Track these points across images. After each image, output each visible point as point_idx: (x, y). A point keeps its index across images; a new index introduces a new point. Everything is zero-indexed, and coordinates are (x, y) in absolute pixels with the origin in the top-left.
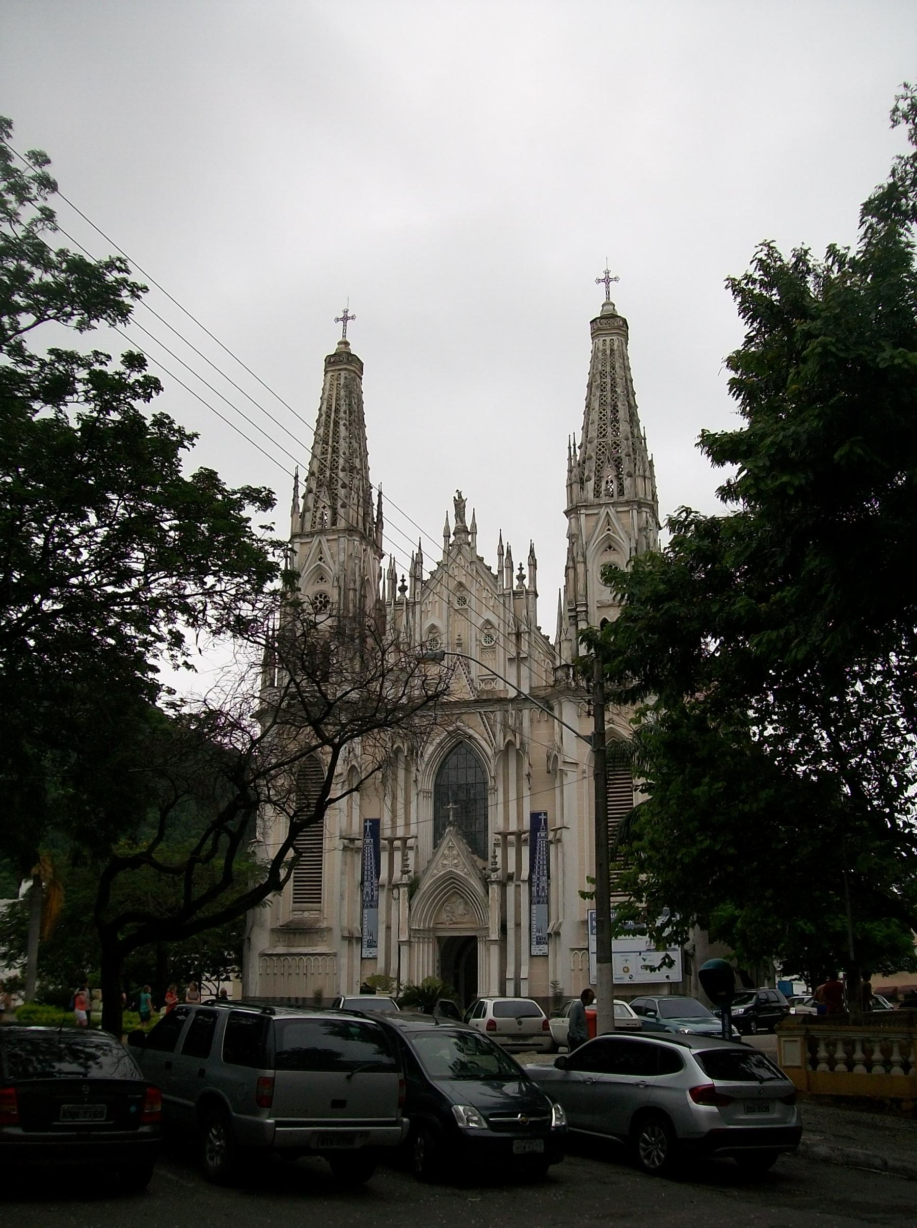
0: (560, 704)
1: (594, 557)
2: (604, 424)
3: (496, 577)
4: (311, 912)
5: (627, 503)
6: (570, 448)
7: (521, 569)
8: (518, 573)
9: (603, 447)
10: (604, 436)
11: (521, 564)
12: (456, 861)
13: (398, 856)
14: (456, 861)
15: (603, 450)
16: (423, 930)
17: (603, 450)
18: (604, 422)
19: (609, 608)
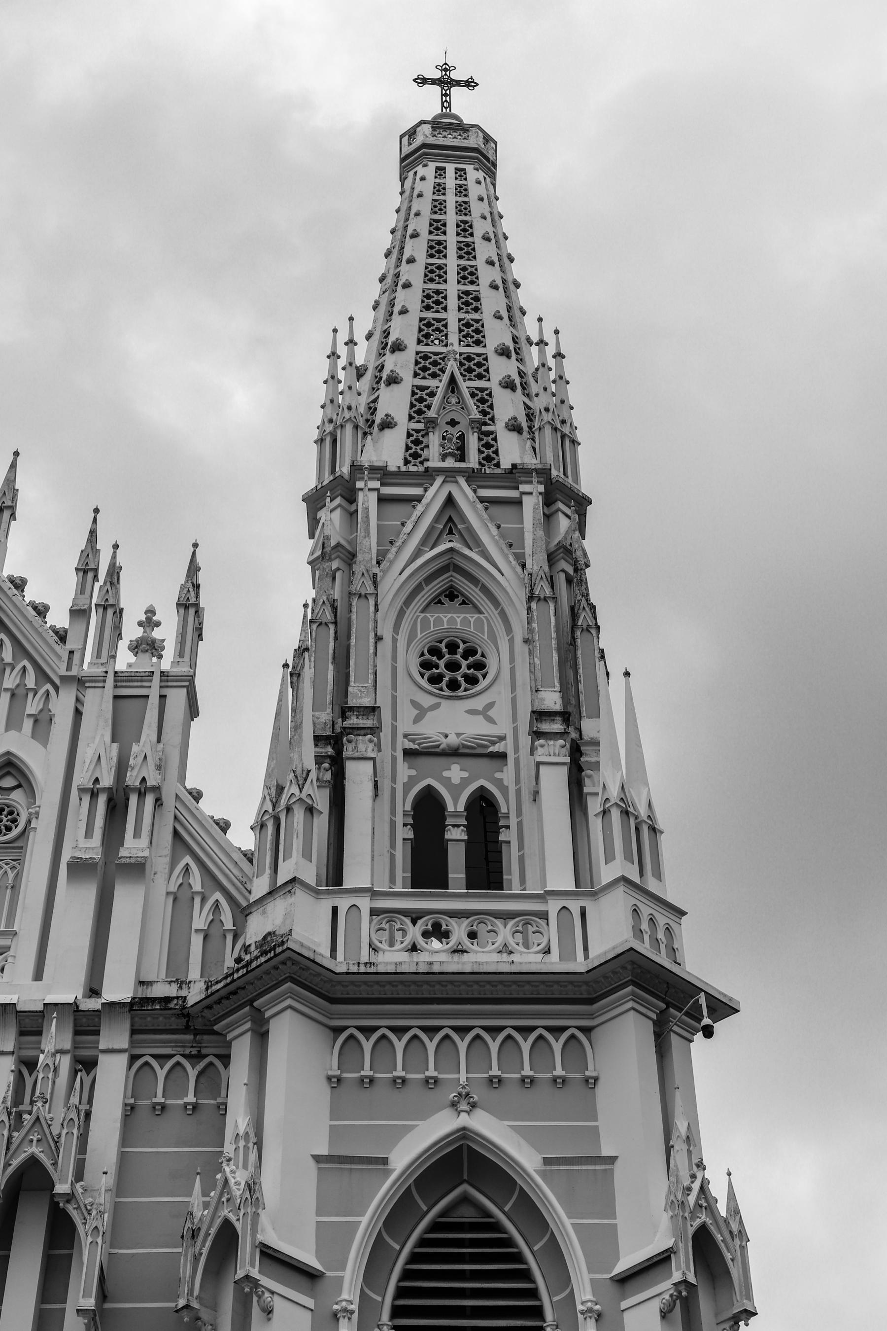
0: (262, 1036)
1: (401, 614)
3: (62, 636)
5: (516, 474)
6: (333, 355)
7: (150, 621)
8: (139, 632)
11: (150, 612)
15: (433, 369)
17: (433, 369)
19: (442, 761)
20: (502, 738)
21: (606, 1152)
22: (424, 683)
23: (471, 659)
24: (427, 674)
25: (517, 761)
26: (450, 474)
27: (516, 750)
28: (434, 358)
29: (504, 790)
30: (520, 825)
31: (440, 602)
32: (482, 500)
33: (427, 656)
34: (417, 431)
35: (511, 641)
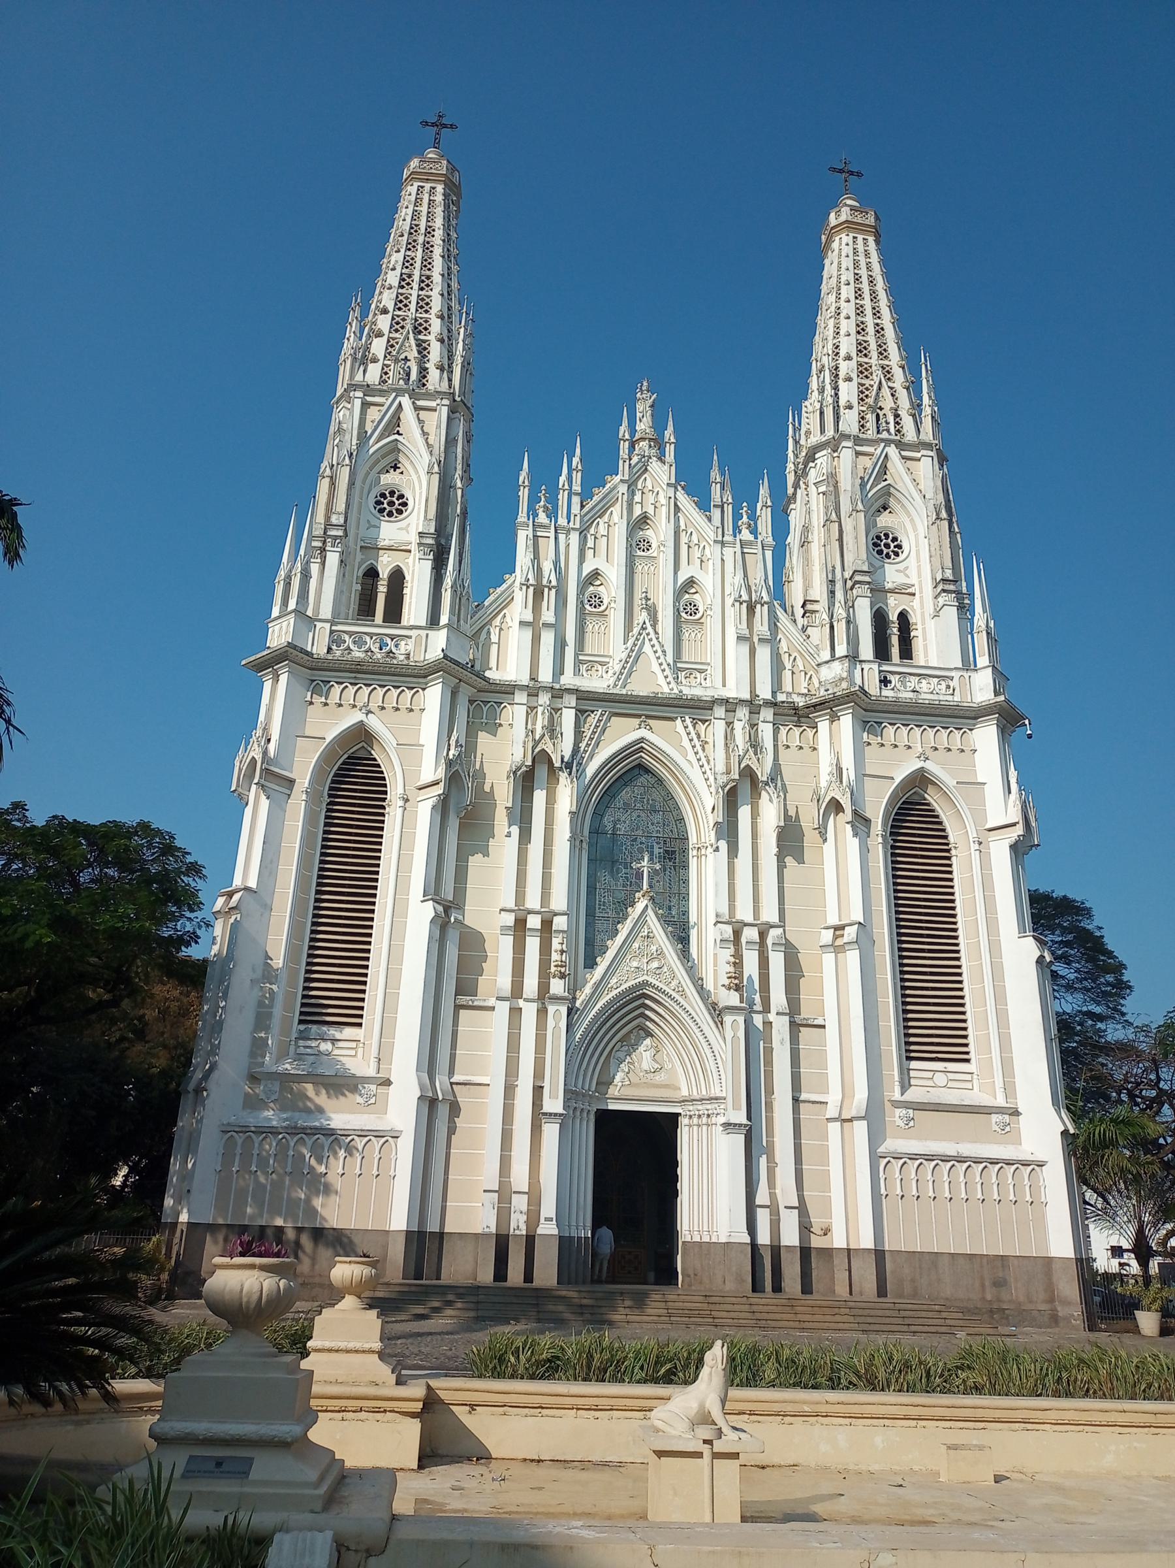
2: (865, 342)
9: (866, 370)
10: (866, 355)
12: (655, 964)
13: (533, 944)
14: (655, 964)
15: (866, 373)
16: (584, 1095)
17: (866, 373)
18: (864, 338)
20: (913, 586)
21: (979, 780)
22: (875, 553)
23: (896, 543)
24: (876, 549)
25: (921, 598)
26: (888, 442)
27: (921, 592)
28: (866, 366)
29: (914, 610)
30: (924, 629)
31: (879, 511)
32: (903, 458)
33: (876, 540)
34: (863, 412)
35: (916, 536)
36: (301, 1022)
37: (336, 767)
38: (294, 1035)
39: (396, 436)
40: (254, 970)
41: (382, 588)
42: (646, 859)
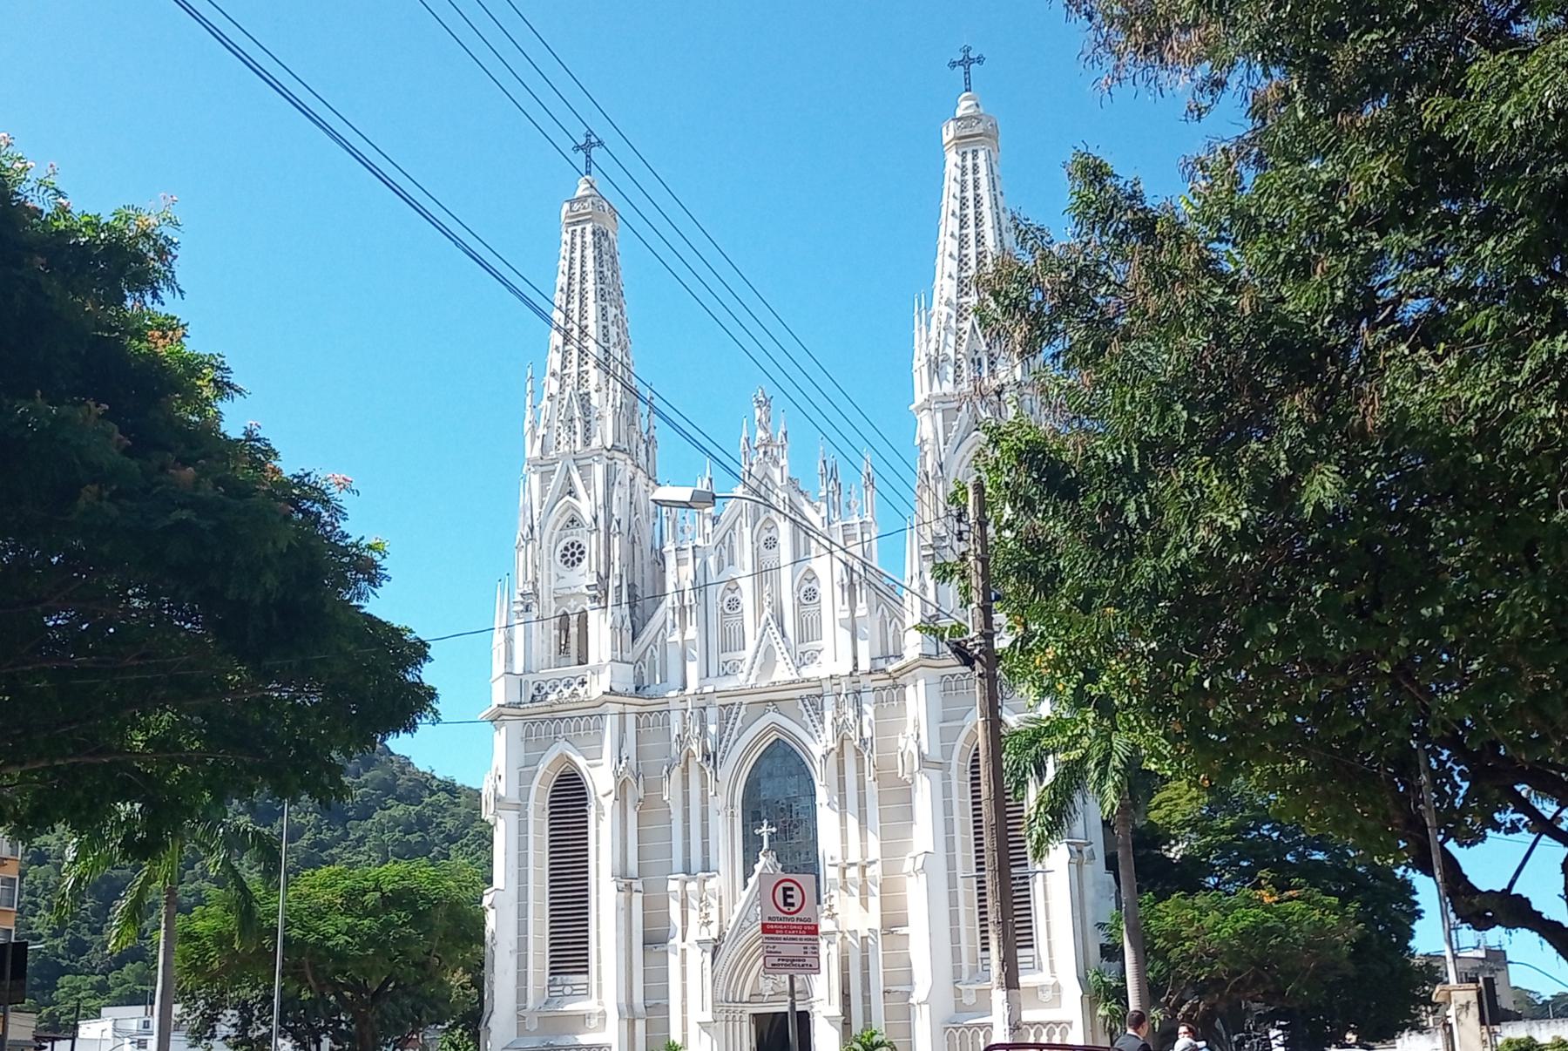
4: (575, 987)
36: (552, 974)
37: (552, 785)
38: (547, 983)
39: (567, 498)
40: (511, 945)
41: (574, 630)
42: (765, 825)
